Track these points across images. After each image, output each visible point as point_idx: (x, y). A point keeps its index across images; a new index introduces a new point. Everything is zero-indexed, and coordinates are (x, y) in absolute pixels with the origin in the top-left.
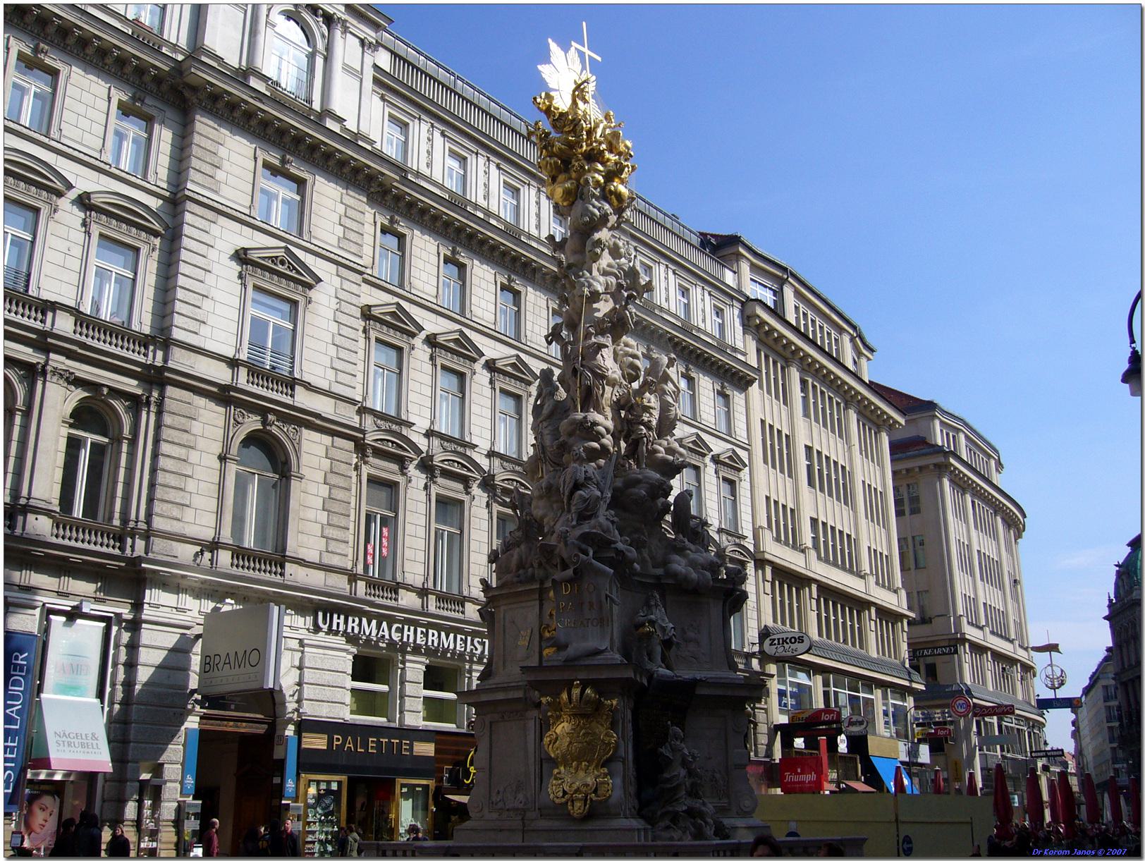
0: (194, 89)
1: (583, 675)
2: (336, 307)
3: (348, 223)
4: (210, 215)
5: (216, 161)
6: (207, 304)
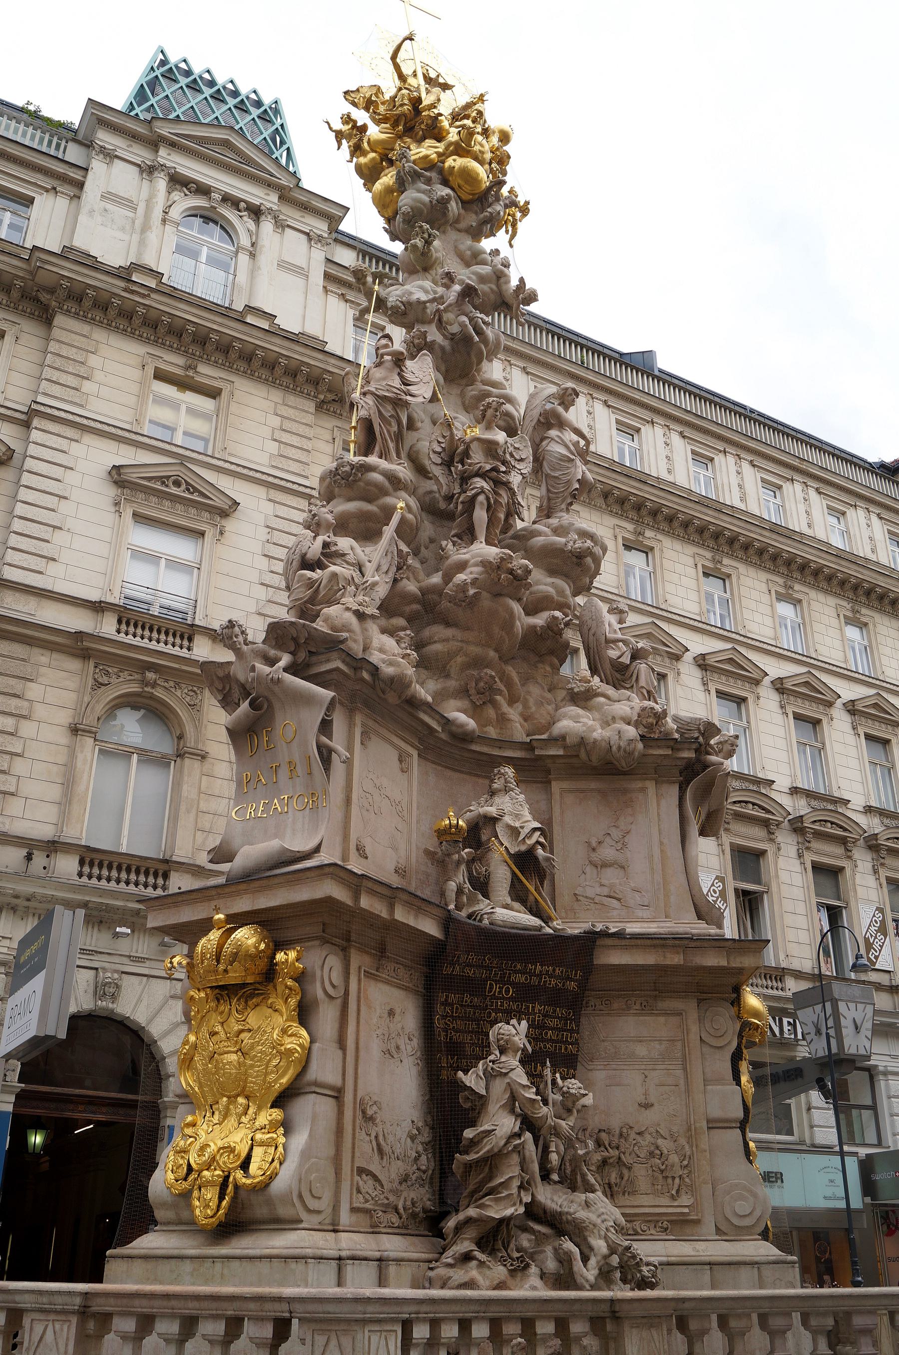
0: (52, 291)
1: (243, 905)
2: (265, 537)
3: (286, 437)
4: (69, 432)
5: (82, 371)
6: (58, 538)
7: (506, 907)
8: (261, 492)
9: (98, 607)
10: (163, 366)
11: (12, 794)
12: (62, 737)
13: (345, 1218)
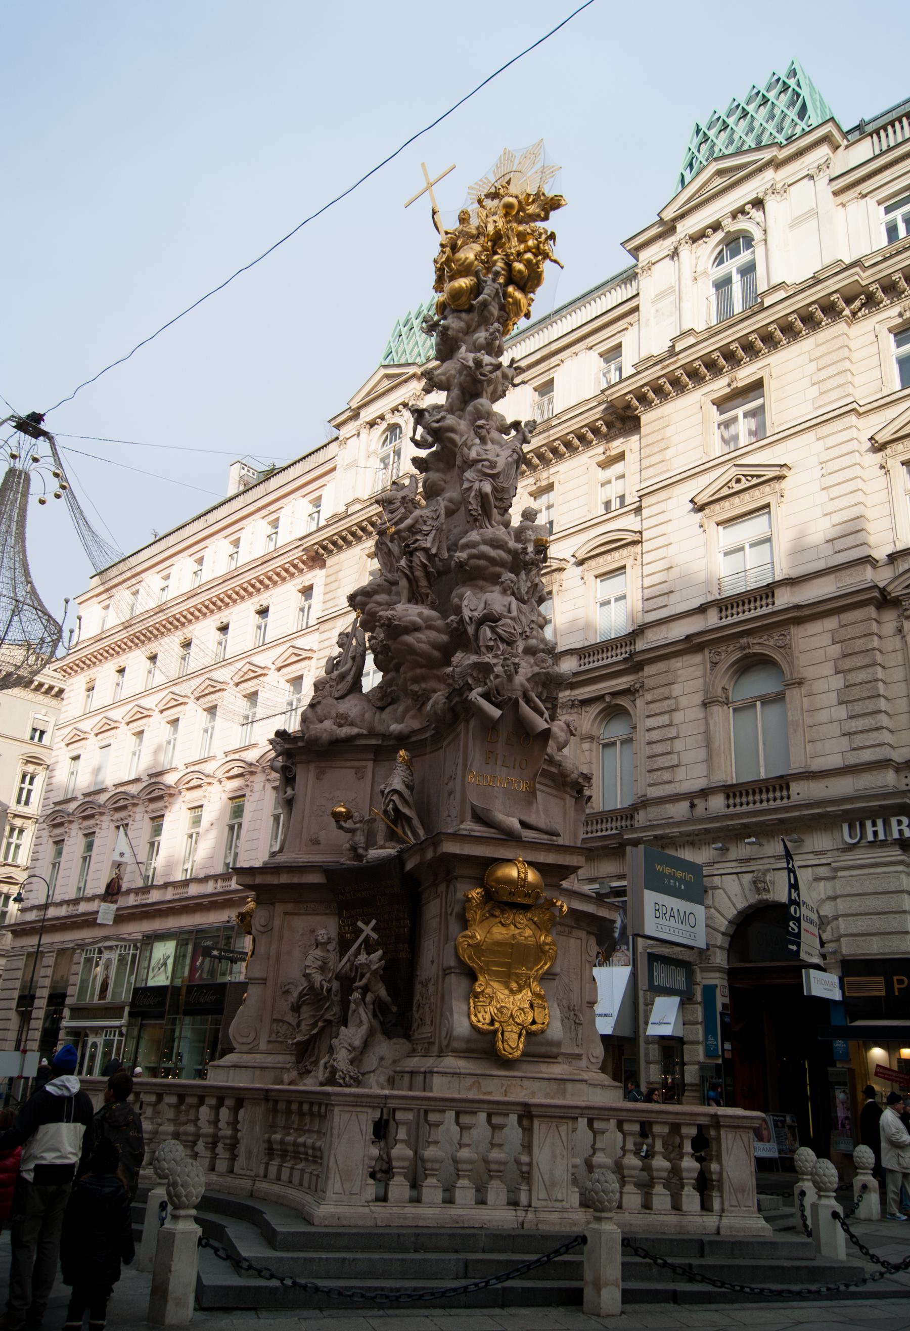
4: (662, 495)
5: (663, 445)
7: (382, 847)
8: (810, 436)
9: (702, 609)
10: (716, 395)
11: (677, 766)
12: (699, 713)
13: (263, 1046)
